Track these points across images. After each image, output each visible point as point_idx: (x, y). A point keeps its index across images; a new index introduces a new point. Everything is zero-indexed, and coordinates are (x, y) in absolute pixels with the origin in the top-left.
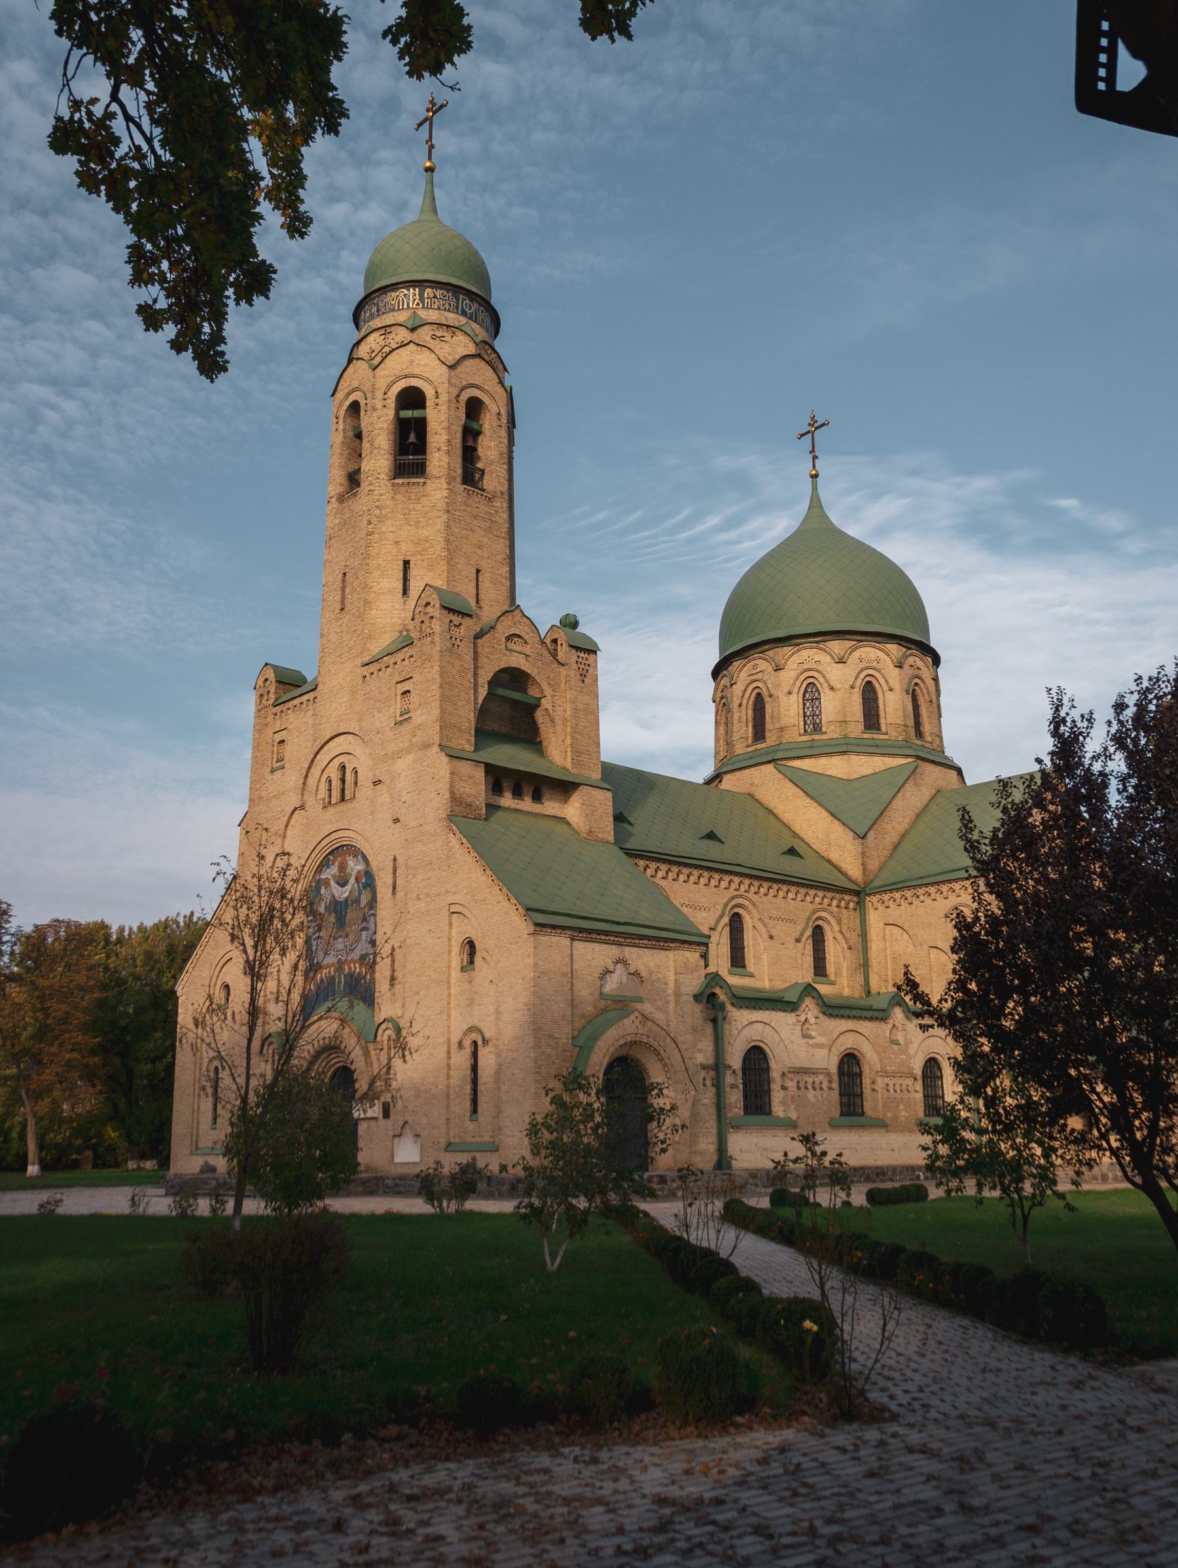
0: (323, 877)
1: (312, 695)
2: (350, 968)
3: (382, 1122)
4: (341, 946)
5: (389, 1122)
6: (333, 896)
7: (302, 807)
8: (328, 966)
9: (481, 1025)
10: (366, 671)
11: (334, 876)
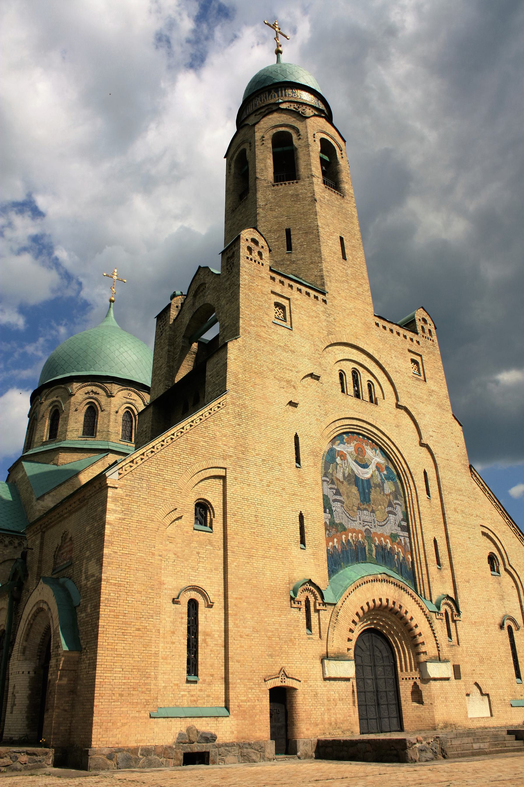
0: (338, 448)
1: (321, 297)
2: (381, 541)
3: (453, 681)
4: (368, 518)
5: (460, 682)
6: (352, 470)
7: (317, 378)
8: (354, 531)
9: (512, 615)
10: (378, 320)
11: (350, 454)
